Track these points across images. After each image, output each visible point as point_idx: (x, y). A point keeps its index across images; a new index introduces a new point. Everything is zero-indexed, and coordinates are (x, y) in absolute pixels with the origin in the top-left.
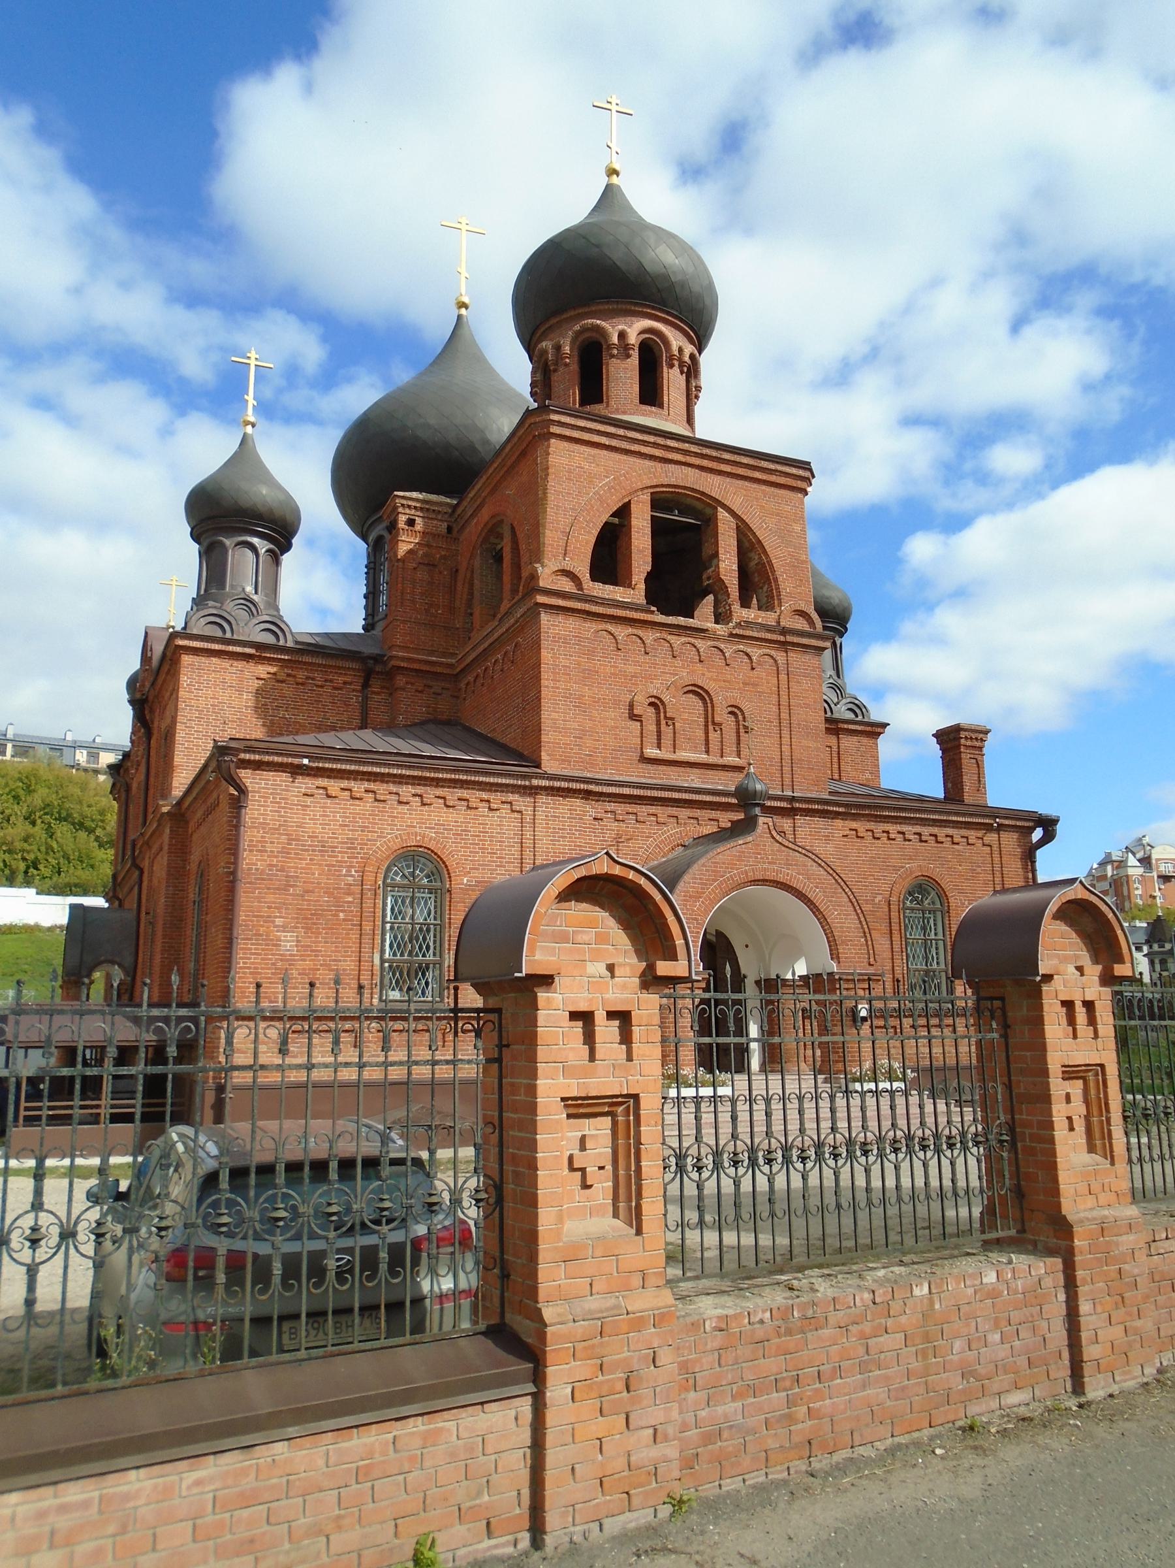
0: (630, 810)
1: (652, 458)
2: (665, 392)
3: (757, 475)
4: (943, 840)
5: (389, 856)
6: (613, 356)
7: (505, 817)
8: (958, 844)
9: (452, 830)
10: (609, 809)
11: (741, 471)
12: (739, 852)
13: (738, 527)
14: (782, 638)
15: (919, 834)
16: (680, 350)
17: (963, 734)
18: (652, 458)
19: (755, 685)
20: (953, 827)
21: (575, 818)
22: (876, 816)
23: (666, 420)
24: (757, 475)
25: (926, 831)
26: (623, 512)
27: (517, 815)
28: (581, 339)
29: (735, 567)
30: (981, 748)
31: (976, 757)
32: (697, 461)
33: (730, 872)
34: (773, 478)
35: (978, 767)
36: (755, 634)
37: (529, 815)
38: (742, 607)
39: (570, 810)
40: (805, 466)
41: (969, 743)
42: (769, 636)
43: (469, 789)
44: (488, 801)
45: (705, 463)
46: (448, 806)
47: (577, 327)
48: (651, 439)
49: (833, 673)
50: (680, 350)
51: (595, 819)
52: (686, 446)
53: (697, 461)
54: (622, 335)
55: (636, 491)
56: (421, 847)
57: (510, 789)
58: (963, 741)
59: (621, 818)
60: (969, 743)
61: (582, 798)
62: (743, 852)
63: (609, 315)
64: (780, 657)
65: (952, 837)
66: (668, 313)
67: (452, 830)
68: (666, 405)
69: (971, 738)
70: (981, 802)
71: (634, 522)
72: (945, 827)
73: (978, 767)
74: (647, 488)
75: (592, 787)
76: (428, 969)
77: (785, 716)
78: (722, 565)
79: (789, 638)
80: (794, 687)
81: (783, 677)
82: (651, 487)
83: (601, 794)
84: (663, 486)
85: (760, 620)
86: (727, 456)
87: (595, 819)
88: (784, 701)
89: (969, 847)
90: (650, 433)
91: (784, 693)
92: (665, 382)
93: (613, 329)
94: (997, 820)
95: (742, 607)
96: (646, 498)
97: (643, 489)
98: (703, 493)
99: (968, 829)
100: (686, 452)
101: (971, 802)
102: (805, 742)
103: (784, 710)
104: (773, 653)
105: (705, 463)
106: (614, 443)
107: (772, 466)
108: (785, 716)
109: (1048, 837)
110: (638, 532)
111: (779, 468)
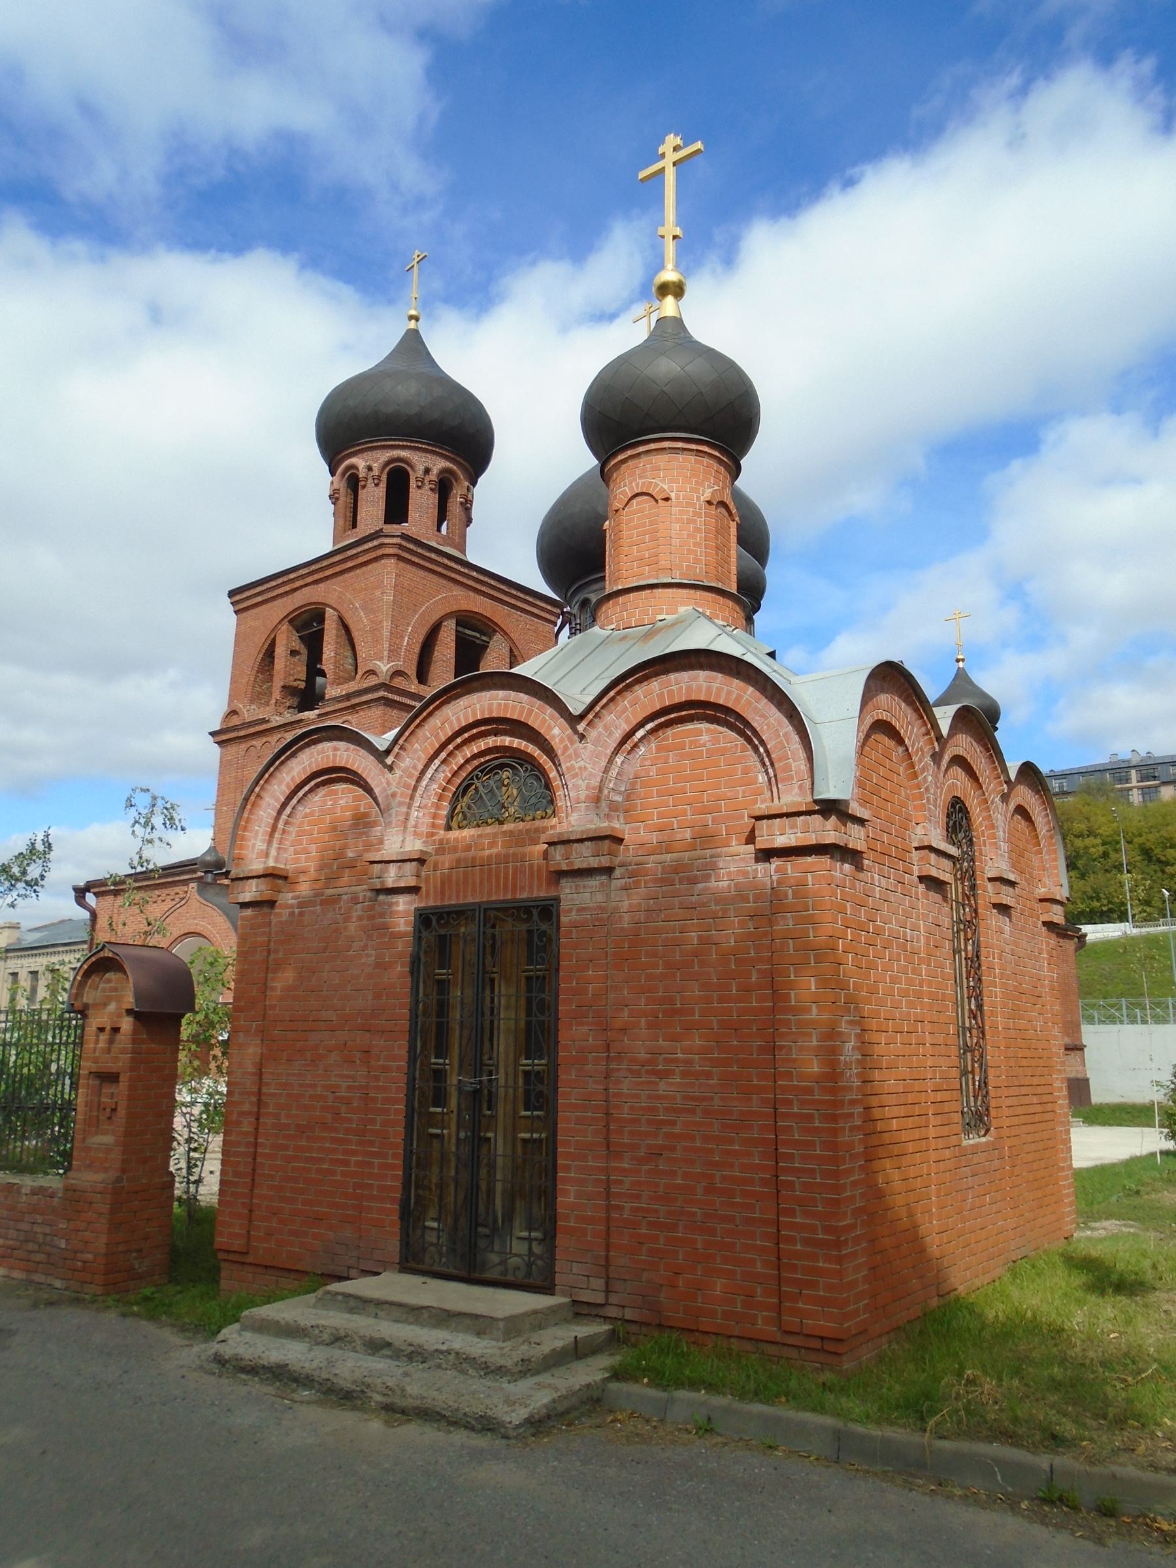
1: (287, 593)
3: (350, 564)
11: (338, 569)
14: (348, 704)
16: (370, 469)
18: (287, 593)
24: (350, 564)
32: (309, 579)
42: (341, 705)
45: (316, 577)
48: (280, 581)
50: (370, 469)
53: (309, 579)
66: (359, 445)
74: (283, 619)
90: (279, 577)
96: (285, 627)
98: (315, 603)
100: (302, 577)
105: (316, 577)
106: (265, 597)
107: (354, 551)
111: (359, 549)
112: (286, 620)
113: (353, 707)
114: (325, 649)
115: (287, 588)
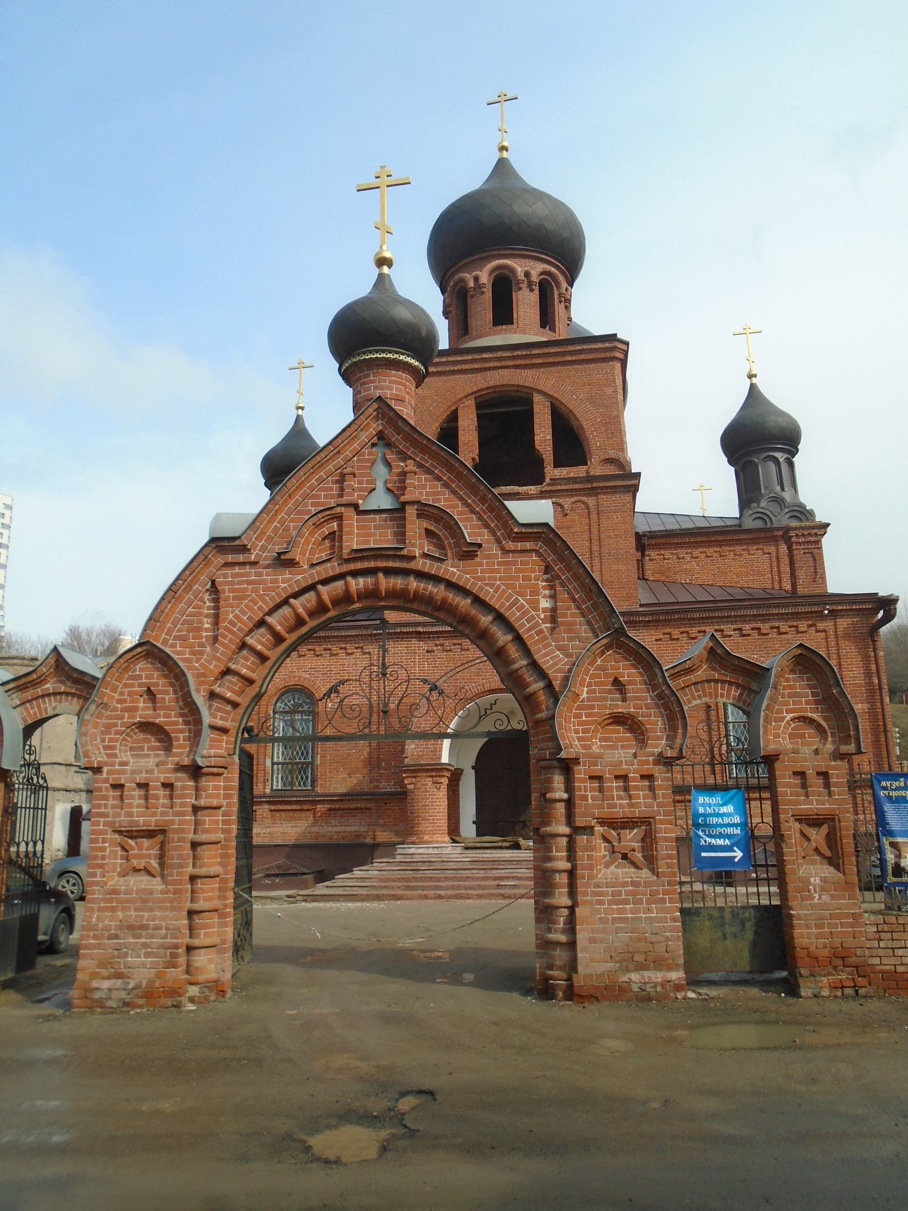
0: (456, 642)
1: (474, 371)
2: (515, 311)
3: (569, 358)
4: (769, 631)
5: (276, 694)
6: (472, 296)
7: (359, 658)
8: (786, 633)
9: (320, 671)
10: (438, 642)
11: (551, 360)
12: (478, 669)
13: (552, 404)
14: (590, 486)
15: (740, 630)
16: (527, 274)
17: (792, 533)
19: (569, 527)
20: (779, 619)
21: (410, 653)
22: (689, 619)
23: (515, 333)
24: (569, 358)
25: (747, 627)
26: (453, 417)
27: (367, 656)
28: (456, 290)
29: (549, 437)
30: (818, 542)
31: (812, 550)
32: (512, 363)
33: (468, 686)
34: (583, 357)
35: (815, 560)
36: (564, 487)
37: (375, 654)
38: (554, 467)
39: (407, 647)
40: (613, 338)
41: (802, 540)
42: (576, 486)
43: (330, 641)
44: (345, 649)
45: (519, 362)
46: (317, 656)
47: (452, 283)
49: (778, 488)
51: (428, 652)
52: (499, 354)
53: (512, 363)
54: (476, 279)
55: (461, 399)
56: (298, 685)
57: (360, 638)
58: (794, 539)
59: (448, 648)
60: (802, 540)
61: (415, 638)
62: (481, 669)
63: (461, 269)
64: (591, 501)
65: (778, 628)
67: (320, 671)
68: (515, 321)
69: (803, 535)
70: (818, 591)
71: (460, 423)
72: (770, 619)
73: (815, 560)
74: (470, 395)
75: (420, 629)
76: (307, 767)
77: (595, 548)
78: (537, 438)
79: (595, 485)
80: (604, 523)
81: (594, 516)
82: (473, 393)
83: (430, 633)
84: (482, 390)
85: (572, 475)
86: (536, 351)
87: (428, 652)
88: (595, 536)
89: (800, 635)
91: (595, 531)
92: (514, 303)
93: (469, 277)
94: (828, 607)
95: (554, 467)
96: (471, 402)
97: (466, 397)
98: (518, 386)
99: (797, 618)
101: (806, 591)
102: (615, 567)
103: (595, 542)
104: (585, 499)
105: (519, 362)
108: (595, 548)
109: (889, 616)
110: (463, 430)
112: (473, 396)
113: (593, 489)
114: (536, 431)
115: (476, 366)
